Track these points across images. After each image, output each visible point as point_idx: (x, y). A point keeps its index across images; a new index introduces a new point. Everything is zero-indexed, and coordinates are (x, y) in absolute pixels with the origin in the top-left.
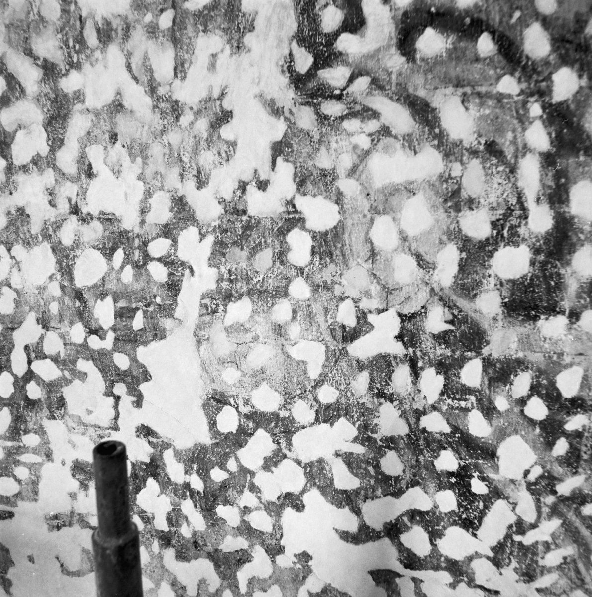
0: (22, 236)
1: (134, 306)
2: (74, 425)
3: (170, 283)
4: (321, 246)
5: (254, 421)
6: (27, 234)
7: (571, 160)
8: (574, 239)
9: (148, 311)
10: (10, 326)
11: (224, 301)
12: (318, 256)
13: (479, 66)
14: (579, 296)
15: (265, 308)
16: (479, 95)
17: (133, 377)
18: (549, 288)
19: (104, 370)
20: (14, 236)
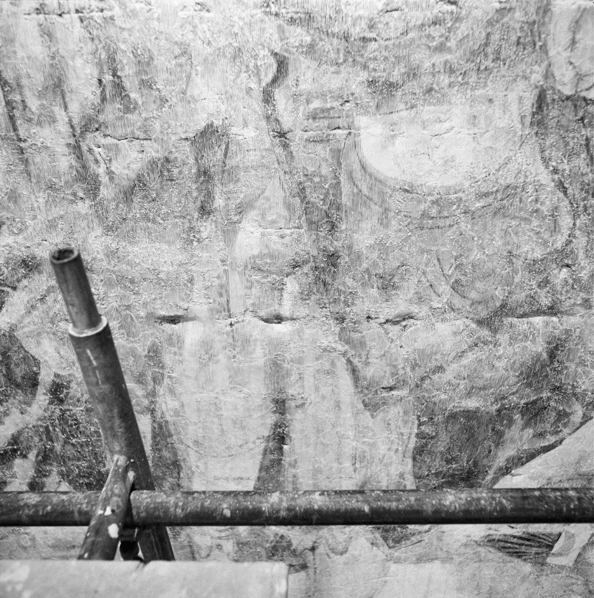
0: (200, 34)
1: (329, 106)
2: (253, 230)
3: (371, 80)
4: (527, 36)
6: (208, 32)
9: (343, 110)
10: (183, 137)
11: (424, 95)
12: (522, 46)
15: (464, 100)
17: (321, 176)
19: (291, 172)
20: (191, 36)
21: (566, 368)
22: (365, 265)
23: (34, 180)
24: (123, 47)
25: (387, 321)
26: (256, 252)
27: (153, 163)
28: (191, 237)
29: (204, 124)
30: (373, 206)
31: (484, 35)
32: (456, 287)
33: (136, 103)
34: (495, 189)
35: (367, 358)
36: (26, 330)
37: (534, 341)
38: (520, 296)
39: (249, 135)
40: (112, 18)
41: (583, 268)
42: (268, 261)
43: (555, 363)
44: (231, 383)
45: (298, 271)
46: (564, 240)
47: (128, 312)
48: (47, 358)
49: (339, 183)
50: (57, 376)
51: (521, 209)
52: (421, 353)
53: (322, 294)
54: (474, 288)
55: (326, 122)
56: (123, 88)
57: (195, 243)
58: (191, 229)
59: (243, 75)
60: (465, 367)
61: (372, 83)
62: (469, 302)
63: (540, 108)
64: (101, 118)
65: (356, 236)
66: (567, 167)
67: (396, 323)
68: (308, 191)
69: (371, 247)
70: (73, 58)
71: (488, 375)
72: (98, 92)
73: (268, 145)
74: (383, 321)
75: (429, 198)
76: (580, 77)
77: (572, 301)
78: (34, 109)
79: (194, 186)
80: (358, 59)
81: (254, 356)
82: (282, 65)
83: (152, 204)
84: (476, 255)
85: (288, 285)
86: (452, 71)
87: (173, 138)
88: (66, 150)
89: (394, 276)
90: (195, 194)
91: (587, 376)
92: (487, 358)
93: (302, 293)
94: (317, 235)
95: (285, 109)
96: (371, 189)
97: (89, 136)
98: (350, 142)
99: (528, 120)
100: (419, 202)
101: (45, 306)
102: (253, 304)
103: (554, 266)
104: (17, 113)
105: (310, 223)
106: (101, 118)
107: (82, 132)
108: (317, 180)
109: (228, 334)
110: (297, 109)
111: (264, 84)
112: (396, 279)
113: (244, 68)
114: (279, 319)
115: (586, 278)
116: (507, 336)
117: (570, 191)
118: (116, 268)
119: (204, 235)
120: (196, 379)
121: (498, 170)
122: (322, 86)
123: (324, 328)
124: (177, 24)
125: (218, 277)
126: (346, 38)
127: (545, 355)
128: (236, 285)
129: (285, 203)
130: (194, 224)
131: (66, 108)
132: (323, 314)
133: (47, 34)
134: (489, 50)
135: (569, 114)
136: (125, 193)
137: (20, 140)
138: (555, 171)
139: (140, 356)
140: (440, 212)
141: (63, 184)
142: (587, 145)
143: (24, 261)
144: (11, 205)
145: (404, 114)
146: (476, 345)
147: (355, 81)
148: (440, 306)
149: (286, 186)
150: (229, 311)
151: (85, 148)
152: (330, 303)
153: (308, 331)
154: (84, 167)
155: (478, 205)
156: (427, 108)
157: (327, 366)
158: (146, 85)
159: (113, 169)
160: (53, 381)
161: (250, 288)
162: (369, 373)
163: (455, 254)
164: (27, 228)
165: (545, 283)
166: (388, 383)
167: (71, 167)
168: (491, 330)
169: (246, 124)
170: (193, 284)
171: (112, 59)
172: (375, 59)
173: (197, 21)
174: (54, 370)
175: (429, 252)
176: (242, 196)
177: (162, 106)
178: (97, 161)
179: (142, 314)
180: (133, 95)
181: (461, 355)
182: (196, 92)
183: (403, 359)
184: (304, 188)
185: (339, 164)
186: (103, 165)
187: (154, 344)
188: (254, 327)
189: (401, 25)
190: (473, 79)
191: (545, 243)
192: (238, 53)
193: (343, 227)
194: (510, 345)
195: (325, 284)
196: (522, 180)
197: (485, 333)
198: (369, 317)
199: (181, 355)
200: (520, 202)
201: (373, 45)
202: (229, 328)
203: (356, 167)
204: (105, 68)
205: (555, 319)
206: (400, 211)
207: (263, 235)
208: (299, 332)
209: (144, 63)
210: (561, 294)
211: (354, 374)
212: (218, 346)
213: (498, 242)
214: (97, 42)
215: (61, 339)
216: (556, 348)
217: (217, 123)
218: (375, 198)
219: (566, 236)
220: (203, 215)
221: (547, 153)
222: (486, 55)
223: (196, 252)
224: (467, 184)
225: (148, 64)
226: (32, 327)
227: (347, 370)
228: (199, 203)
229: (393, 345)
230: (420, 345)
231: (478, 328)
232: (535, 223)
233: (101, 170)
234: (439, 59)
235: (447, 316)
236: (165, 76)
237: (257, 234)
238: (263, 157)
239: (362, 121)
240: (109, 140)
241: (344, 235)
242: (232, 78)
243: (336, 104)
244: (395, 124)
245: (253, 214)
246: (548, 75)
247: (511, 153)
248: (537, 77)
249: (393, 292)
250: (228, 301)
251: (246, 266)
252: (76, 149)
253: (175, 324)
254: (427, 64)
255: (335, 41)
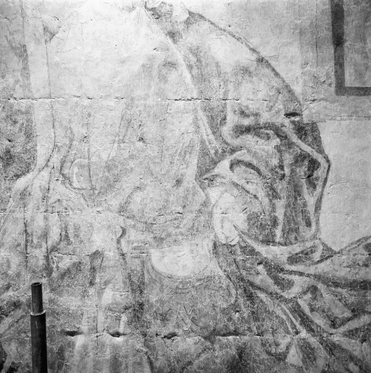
1: (140, 245)
2: (109, 292)
5: (182, 284)
7: (276, 201)
8: (278, 222)
13: (251, 175)
14: (280, 238)
16: (251, 182)
18: (272, 235)
20: (94, 221)
21: (249, 364)
22: (154, 309)
23: (28, 269)
24: (71, 223)
25: (165, 337)
26: (110, 302)
27: (74, 264)
28: (84, 295)
29: (95, 250)
30: (157, 284)
31: (192, 223)
32: (193, 320)
33: (72, 242)
34: (203, 278)
35: (157, 356)
36: (6, 337)
37: (230, 348)
38: (221, 325)
39: (111, 254)
40: (69, 215)
41: (244, 313)
42: (115, 306)
43: (243, 361)
44: (94, 369)
45: (127, 311)
46: (234, 300)
47: (53, 329)
48: (11, 353)
49: (144, 274)
50: (13, 363)
51: (215, 286)
52: (181, 353)
53: (137, 322)
54: (201, 321)
55: (139, 251)
56: (68, 237)
57: (86, 297)
58: (85, 291)
59: (111, 234)
60: (202, 362)
61: (155, 238)
62: (199, 328)
63: (215, 247)
64: (58, 247)
65: (150, 296)
66: (229, 269)
67: (169, 338)
68: (132, 276)
69: (156, 301)
70: (53, 226)
71: (213, 367)
72: (59, 238)
73: (117, 258)
74: (163, 336)
75: (178, 281)
76: (227, 238)
77: (243, 328)
78: (35, 243)
79: (89, 273)
80: (150, 230)
81: (106, 353)
82: (124, 232)
83: (71, 280)
84: (200, 306)
85: (123, 318)
86: (182, 235)
87: (83, 255)
88: (43, 258)
89: (167, 315)
90: (89, 276)
91: (259, 369)
92: (211, 357)
93: (128, 322)
94: (135, 295)
95: (124, 246)
96: (156, 276)
97: (53, 253)
98: (148, 258)
99: (212, 252)
100: (175, 282)
101: (17, 325)
102: (107, 327)
103: (232, 311)
104: (29, 244)
105: (133, 290)
106: (58, 247)
107: (50, 252)
108: (135, 272)
109: (95, 341)
110: (129, 246)
111: (117, 237)
112: (168, 316)
113: (111, 232)
114: (117, 334)
115: (246, 317)
116: (218, 346)
117: (232, 279)
118: (52, 307)
119: (90, 294)
120: (78, 366)
121: (203, 270)
122: (138, 238)
123: (138, 339)
124: (90, 217)
125: (94, 313)
126: (146, 223)
127: (237, 356)
128: (101, 317)
129: (123, 281)
130: (87, 289)
131: (47, 243)
132: (137, 332)
133: (46, 218)
134: (194, 228)
135: (225, 249)
136: (62, 275)
137: (27, 253)
138: (225, 271)
139: (54, 353)
140: (183, 286)
141: (39, 271)
142: (235, 261)
143: (15, 303)
144: (16, 278)
145: (167, 248)
146: (205, 350)
147: (149, 237)
148: (187, 329)
149: (123, 274)
150: (97, 329)
151: (50, 257)
152: (140, 327)
153: (130, 341)
154: (48, 264)
155: (197, 284)
156: (175, 247)
157: (139, 360)
158: (77, 236)
159: (59, 265)
160: (10, 366)
161: (107, 318)
162: (157, 364)
163: (191, 305)
164: (20, 288)
165: (230, 319)
166: (167, 370)
167: (43, 264)
168: (211, 342)
169: (110, 251)
170: (83, 316)
171: (66, 227)
172: (156, 230)
173: (96, 216)
174: (12, 360)
175: (180, 304)
176: (106, 278)
177: (81, 243)
178: (54, 262)
179: (59, 330)
180: (71, 239)
181: (199, 356)
182: (93, 239)
183: (173, 357)
184: (130, 275)
185: (144, 266)
186: (55, 264)
187: (62, 345)
188: (107, 338)
189: (164, 220)
190: (190, 237)
191: (227, 301)
192: (109, 227)
193: (146, 292)
194: (220, 350)
195: (138, 317)
196: (213, 274)
197: (208, 344)
198: (157, 335)
199: (73, 352)
200: (214, 283)
201: (155, 226)
202: (96, 338)
203: (150, 268)
204: (63, 230)
205: (238, 337)
206: (167, 286)
207: (114, 295)
208: (127, 341)
209: (77, 229)
210: (238, 325)
211: (151, 365)
212: (90, 348)
213: (208, 300)
214: (62, 222)
215: (20, 342)
216: (241, 352)
217: (100, 250)
218: (158, 280)
219: (234, 298)
220: (91, 285)
221: (221, 264)
222: (193, 230)
223: (86, 301)
224: (192, 275)
225: (78, 229)
226: (9, 336)
227: (148, 362)
228: (90, 280)
229: (168, 349)
230: (180, 349)
231: (205, 341)
232: (221, 292)
233: (54, 266)
234: (178, 231)
235: (191, 334)
236: (83, 233)
237: (111, 294)
238: (116, 263)
239: (152, 251)
240: (60, 255)
241: (146, 296)
242: (106, 235)
243: (142, 245)
244: (164, 252)
245: (110, 286)
246: (216, 236)
247: (207, 264)
248: (212, 237)
249: (167, 322)
250: (97, 325)
251: (106, 308)
252: (47, 258)
253: (73, 336)
254: (174, 232)
255: (142, 224)
